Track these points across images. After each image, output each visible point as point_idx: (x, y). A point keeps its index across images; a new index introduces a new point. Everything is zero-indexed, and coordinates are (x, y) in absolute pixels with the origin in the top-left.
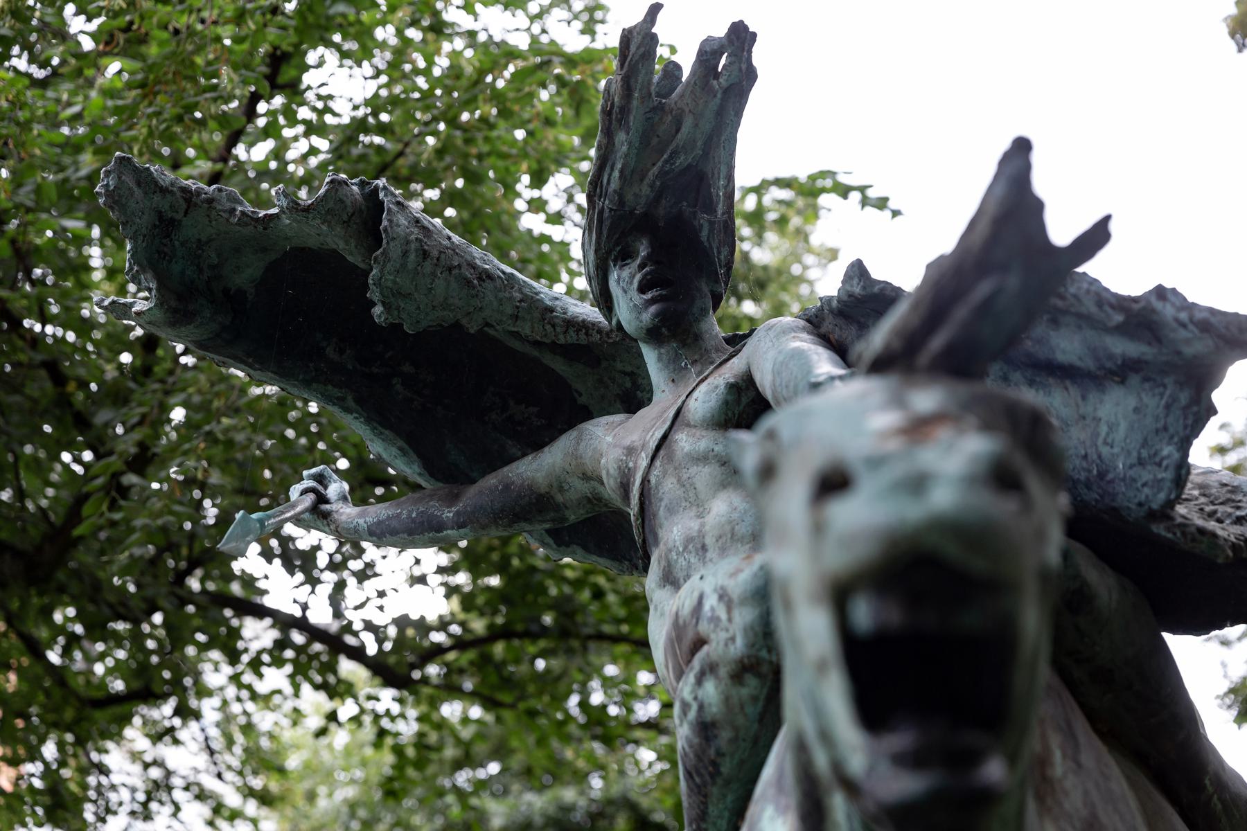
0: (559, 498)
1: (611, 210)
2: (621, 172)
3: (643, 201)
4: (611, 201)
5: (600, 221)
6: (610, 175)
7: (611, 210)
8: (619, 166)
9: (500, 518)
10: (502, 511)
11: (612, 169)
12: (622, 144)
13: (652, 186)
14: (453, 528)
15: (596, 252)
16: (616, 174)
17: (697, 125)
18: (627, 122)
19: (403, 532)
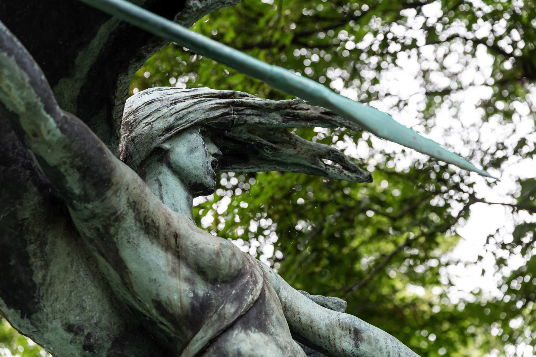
0: (109, 193)
1: (233, 121)
2: (260, 123)
3: (237, 135)
4: (238, 119)
5: (223, 115)
6: (253, 115)
7: (233, 121)
8: (262, 120)
9: (82, 159)
10: (90, 158)
11: (257, 115)
12: (276, 120)
13: (249, 139)
14: (57, 122)
15: (207, 119)
16: (257, 119)
17: (290, 156)
18: (289, 120)
19: (30, 75)
